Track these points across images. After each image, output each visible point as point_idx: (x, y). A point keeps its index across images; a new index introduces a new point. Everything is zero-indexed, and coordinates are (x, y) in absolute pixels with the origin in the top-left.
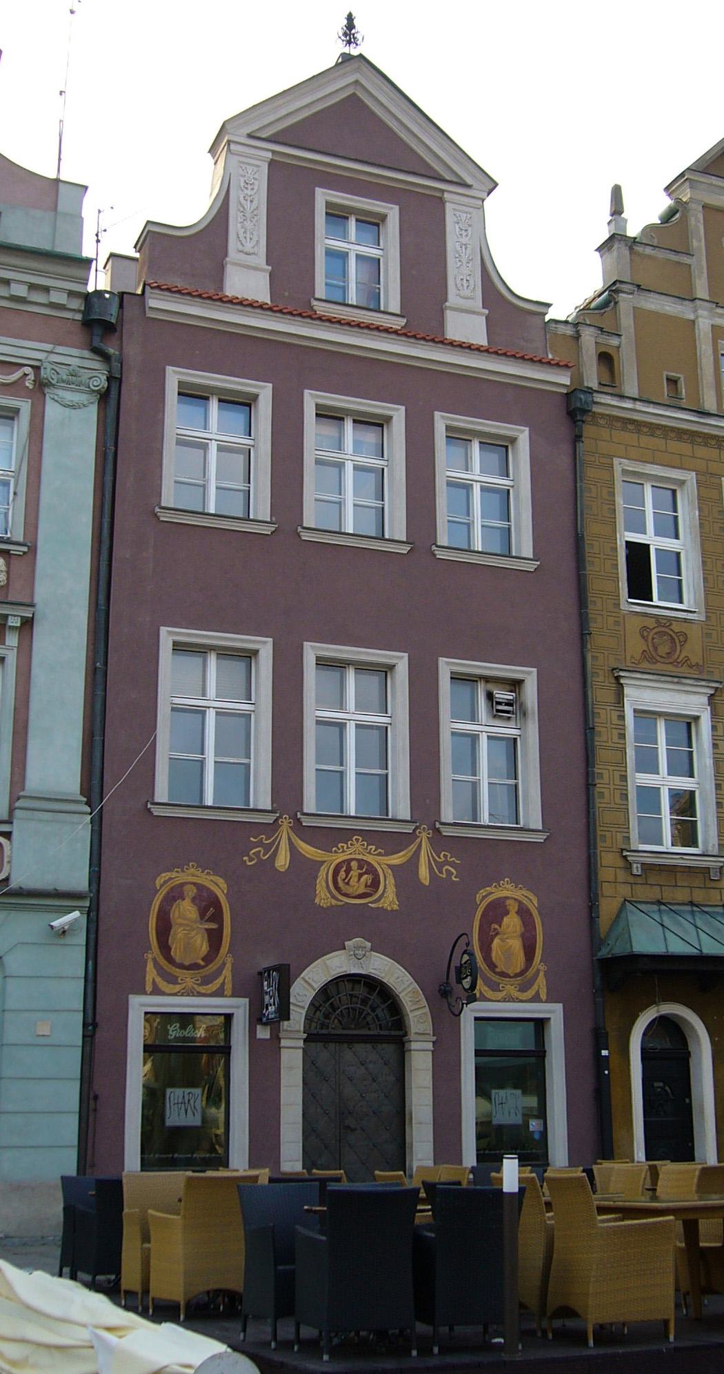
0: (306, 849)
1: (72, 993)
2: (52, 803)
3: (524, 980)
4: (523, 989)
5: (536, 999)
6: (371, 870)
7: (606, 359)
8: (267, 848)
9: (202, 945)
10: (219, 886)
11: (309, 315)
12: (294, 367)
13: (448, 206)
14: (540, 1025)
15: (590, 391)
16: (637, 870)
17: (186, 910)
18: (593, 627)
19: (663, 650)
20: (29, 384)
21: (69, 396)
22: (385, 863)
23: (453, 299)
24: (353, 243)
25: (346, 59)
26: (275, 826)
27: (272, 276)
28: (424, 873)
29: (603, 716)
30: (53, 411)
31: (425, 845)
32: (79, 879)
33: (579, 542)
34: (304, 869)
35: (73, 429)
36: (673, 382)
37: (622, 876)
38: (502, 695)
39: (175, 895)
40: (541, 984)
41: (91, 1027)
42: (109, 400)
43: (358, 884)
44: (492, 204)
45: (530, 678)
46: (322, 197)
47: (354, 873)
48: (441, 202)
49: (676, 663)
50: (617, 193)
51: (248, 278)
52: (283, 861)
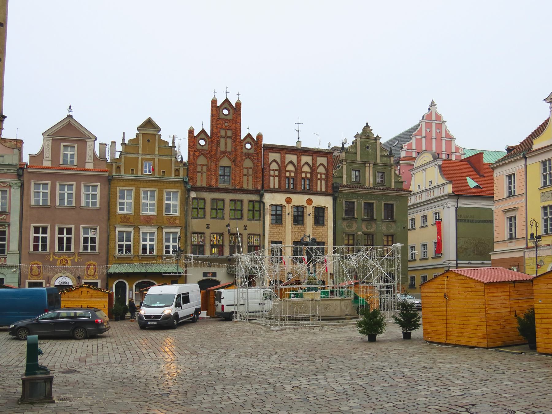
0: (55, 257)
2: (13, 253)
6: (67, 260)
7: (118, 168)
23: (87, 161)
24: (69, 151)
26: (50, 254)
28: (76, 260)
30: (12, 190)
33: (109, 203)
35: (16, 193)
40: (97, 277)
46: (62, 144)
52: (51, 259)
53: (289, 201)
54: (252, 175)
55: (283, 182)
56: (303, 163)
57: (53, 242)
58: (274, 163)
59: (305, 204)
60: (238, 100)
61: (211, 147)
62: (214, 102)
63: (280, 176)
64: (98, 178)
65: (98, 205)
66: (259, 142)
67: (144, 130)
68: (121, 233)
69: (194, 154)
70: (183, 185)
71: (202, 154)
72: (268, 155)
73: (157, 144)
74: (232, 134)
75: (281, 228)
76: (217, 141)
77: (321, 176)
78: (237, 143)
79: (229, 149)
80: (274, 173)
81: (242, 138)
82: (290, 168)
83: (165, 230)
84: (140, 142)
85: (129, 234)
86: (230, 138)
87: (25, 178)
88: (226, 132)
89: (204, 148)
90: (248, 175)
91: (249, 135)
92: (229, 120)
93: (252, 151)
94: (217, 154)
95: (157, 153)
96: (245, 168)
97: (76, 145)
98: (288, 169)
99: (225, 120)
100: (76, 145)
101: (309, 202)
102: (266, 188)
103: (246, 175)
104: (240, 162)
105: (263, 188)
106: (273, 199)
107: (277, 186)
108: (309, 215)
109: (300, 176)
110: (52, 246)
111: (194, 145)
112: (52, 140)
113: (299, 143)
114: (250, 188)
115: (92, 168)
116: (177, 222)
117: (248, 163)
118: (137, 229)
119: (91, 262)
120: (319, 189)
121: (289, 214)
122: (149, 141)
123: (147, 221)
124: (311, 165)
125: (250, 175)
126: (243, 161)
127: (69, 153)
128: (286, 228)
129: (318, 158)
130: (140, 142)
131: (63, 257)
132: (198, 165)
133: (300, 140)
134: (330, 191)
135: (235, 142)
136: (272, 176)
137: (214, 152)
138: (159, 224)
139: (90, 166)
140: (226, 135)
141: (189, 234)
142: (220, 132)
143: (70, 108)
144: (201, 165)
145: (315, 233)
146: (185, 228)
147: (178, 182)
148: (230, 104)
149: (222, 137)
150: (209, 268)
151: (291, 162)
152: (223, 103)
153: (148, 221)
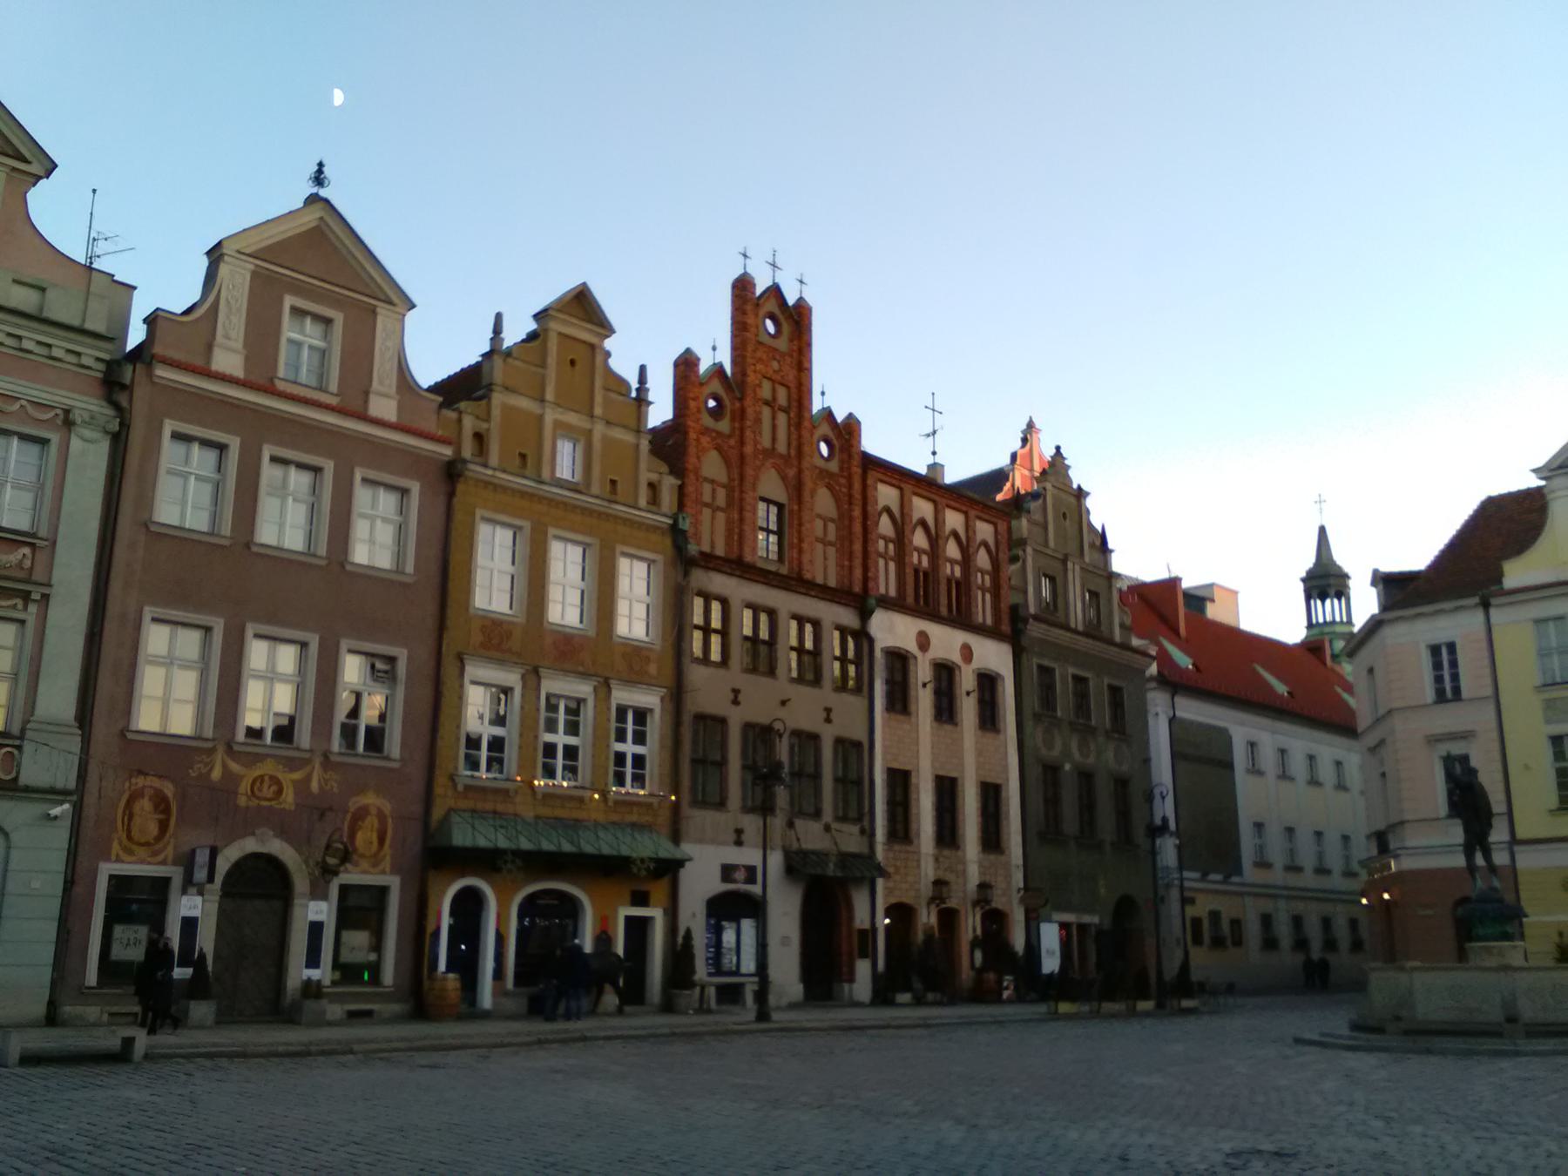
0: (234, 767)
1: (56, 862)
3: (376, 860)
4: (375, 865)
5: (383, 872)
7: (479, 438)
8: (206, 764)
9: (153, 829)
10: (169, 789)
11: (271, 391)
12: (258, 426)
13: (380, 319)
14: (383, 891)
15: (465, 462)
16: (460, 788)
18: (449, 623)
20: (59, 422)
21: (87, 433)
22: (289, 778)
25: (313, 199)
27: (247, 359)
28: (315, 786)
30: (75, 444)
31: (317, 765)
34: (230, 779)
35: (89, 456)
36: (523, 456)
37: (450, 793)
38: (379, 665)
39: (135, 796)
40: (387, 864)
41: (69, 884)
42: (119, 441)
43: (267, 791)
44: (411, 318)
45: (402, 654)
46: (289, 301)
47: (266, 785)
48: (373, 312)
50: (499, 317)
51: (229, 360)
52: (216, 774)
53: (924, 641)
64: (413, 463)
65: (410, 569)
67: (565, 322)
70: (668, 541)
73: (598, 383)
92: (783, 355)
93: (833, 466)
95: (598, 411)
96: (819, 516)
108: (968, 694)
112: (254, 274)
119: (370, 799)
127: (302, 344)
131: (267, 768)
132: (706, 479)
133: (938, 459)
134: (1006, 628)
139: (384, 407)
144: (712, 482)
146: (677, 695)
147: (653, 528)
150: (736, 849)
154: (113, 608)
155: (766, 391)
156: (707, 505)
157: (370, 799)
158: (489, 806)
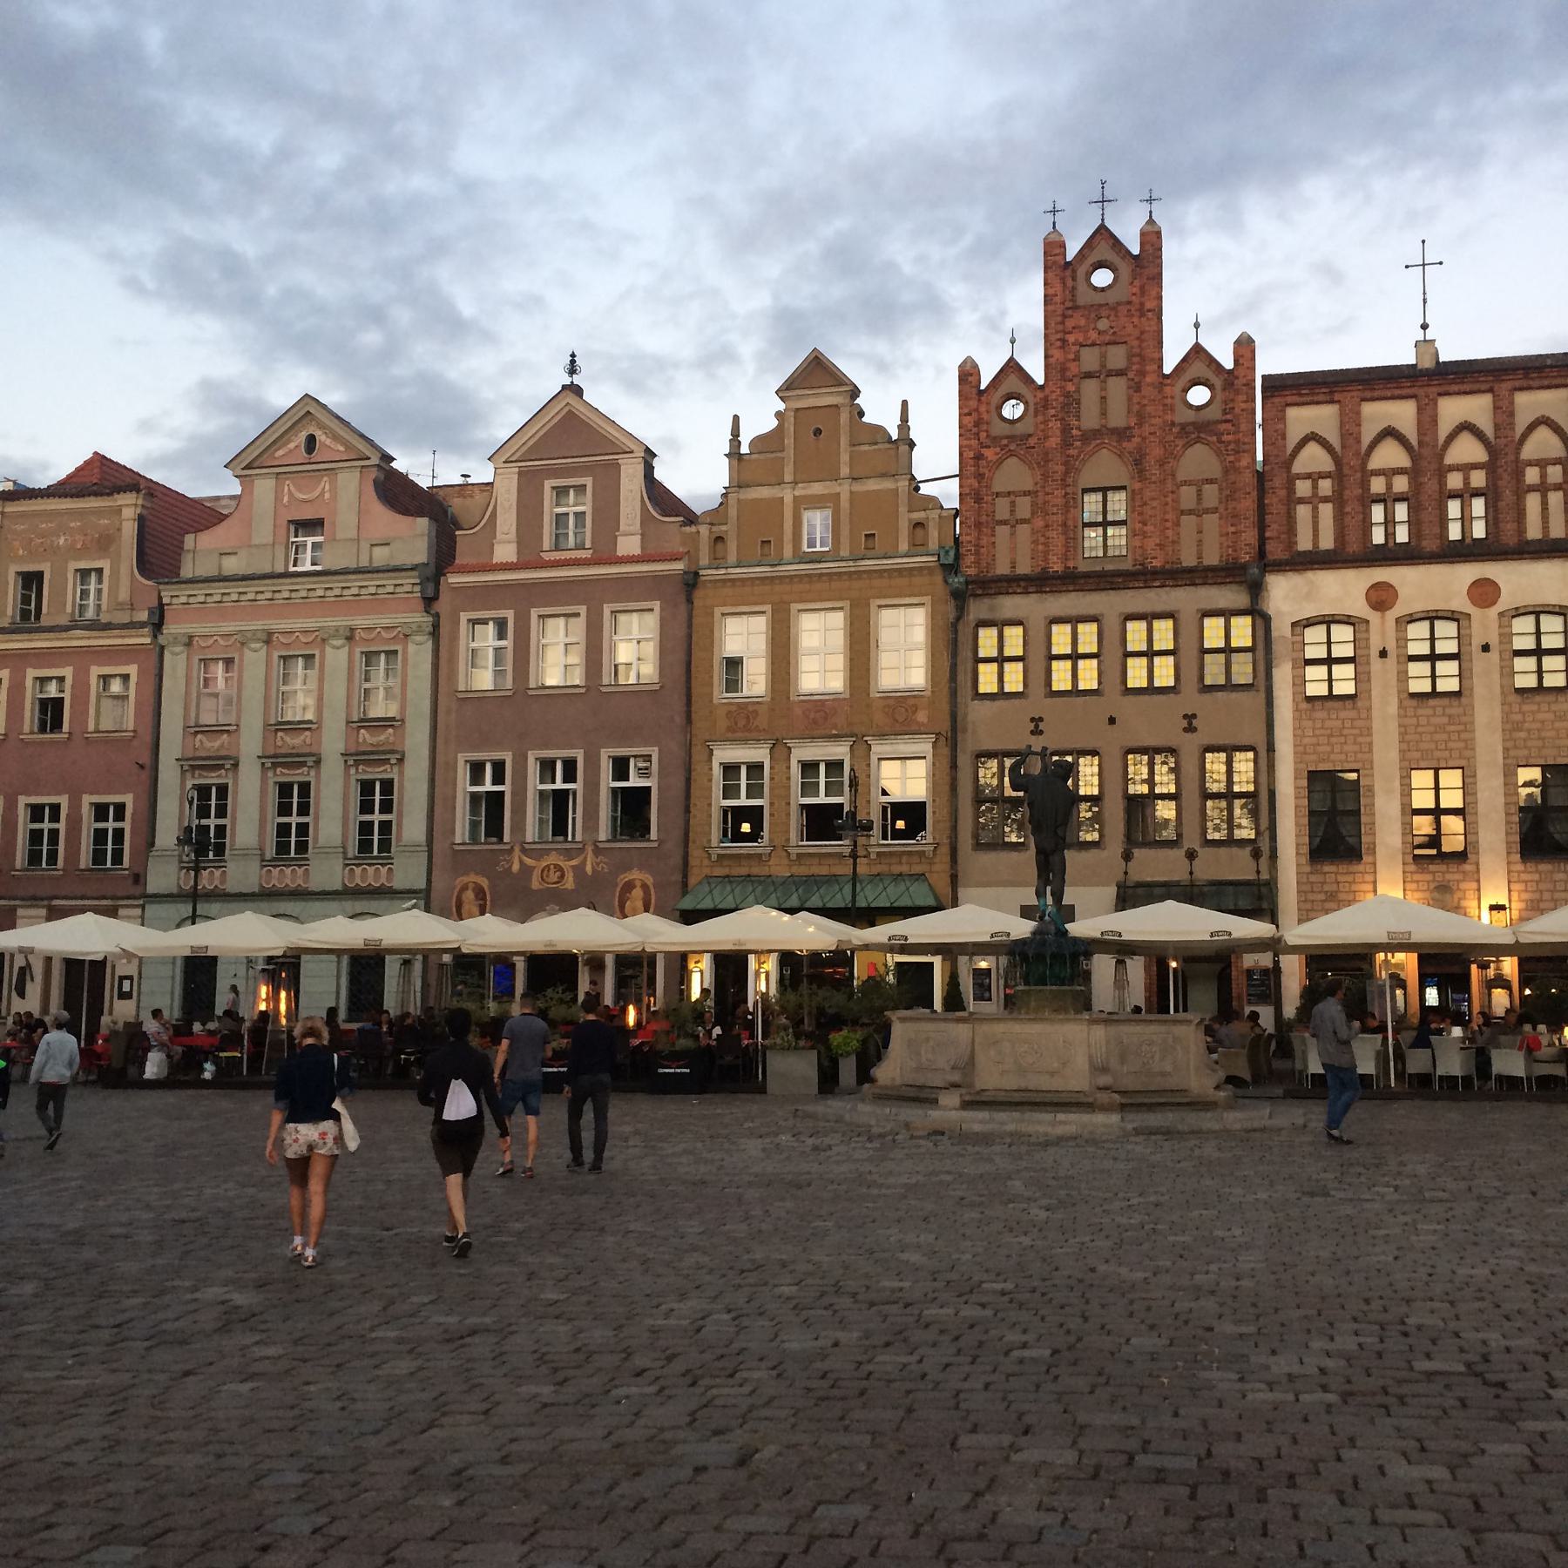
0: (528, 861)
2: (412, 848)
10: (484, 883)
17: (469, 895)
19: (741, 723)
21: (418, 638)
22: (567, 865)
28: (589, 869)
29: (698, 768)
30: (411, 648)
31: (590, 856)
32: (422, 885)
34: (526, 871)
35: (419, 654)
37: (706, 862)
39: (464, 888)
43: (554, 877)
45: (654, 752)
49: (749, 731)
50: (736, 419)
52: (516, 867)
53: (1381, 598)
54: (1215, 511)
55: (1352, 522)
56: (1444, 429)
57: (519, 810)
58: (1313, 449)
59: (1461, 603)
60: (1151, 221)
61: (1045, 422)
62: (1053, 248)
63: (1338, 499)
66: (1241, 372)
68: (730, 770)
69: (979, 457)
70: (939, 578)
71: (1012, 454)
72: (1283, 419)
73: (844, 441)
74: (1130, 356)
75: (1353, 714)
76: (1067, 395)
77: (1543, 476)
78: (1147, 391)
79: (1118, 418)
80: (1315, 487)
81: (1168, 368)
82: (1390, 455)
83: (878, 749)
84: (789, 441)
85: (755, 769)
86: (1120, 373)
87: (442, 606)
88: (1103, 356)
89: (1020, 429)
90: (1197, 513)
91: (1197, 352)
92: (1114, 308)
94: (1066, 443)
95: (845, 471)
96: (1185, 483)
97: (588, 481)
98: (1376, 462)
99: (1096, 311)
100: (588, 481)
101: (1484, 592)
102: (1275, 551)
103: (1190, 512)
104: (1161, 463)
105: (1262, 553)
106: (1308, 596)
107: (1327, 542)
108: (1486, 648)
109: (1431, 486)
110: (519, 826)
111: (977, 424)
113: (1425, 345)
114: (1212, 559)
115: (637, 551)
116: (922, 716)
117: (1198, 461)
118: (780, 749)
120: (1533, 532)
121: (1383, 654)
122: (818, 432)
123: (815, 722)
124: (1489, 430)
125: (1207, 511)
126: (1177, 458)
128: (1375, 713)
129: (1522, 399)
130: (789, 441)
132: (998, 495)
135: (1138, 389)
136: (1302, 501)
137: (1054, 442)
138: (856, 731)
140: (1103, 365)
141: (964, 760)
142: (1077, 359)
143: (573, 362)
145: (1518, 727)
148: (1116, 243)
149: (1089, 375)
151: (1390, 433)
152: (1089, 244)
153: (820, 716)
154: (440, 759)
155: (1090, 359)
156: (1004, 523)
157: (635, 875)
158: (744, 871)
